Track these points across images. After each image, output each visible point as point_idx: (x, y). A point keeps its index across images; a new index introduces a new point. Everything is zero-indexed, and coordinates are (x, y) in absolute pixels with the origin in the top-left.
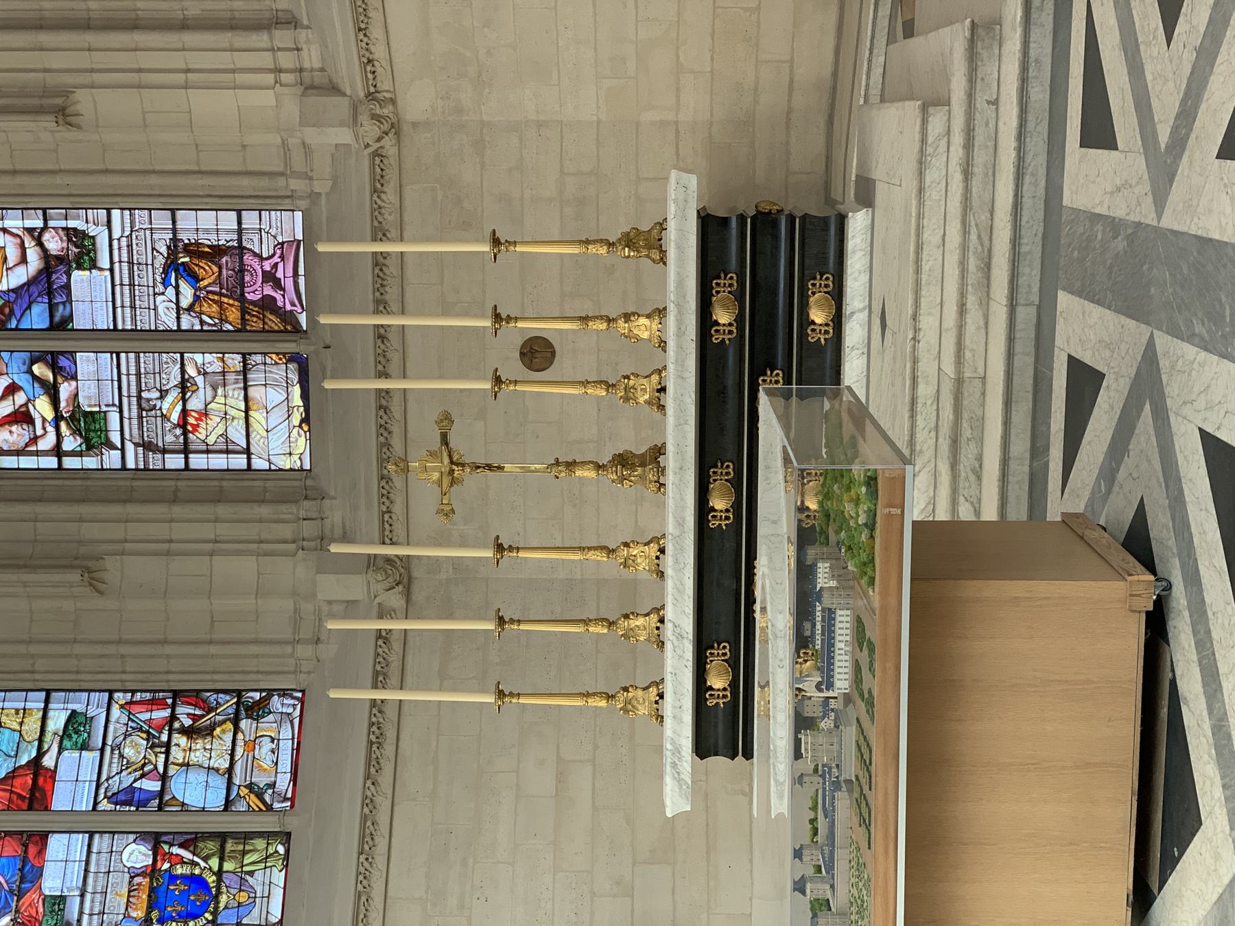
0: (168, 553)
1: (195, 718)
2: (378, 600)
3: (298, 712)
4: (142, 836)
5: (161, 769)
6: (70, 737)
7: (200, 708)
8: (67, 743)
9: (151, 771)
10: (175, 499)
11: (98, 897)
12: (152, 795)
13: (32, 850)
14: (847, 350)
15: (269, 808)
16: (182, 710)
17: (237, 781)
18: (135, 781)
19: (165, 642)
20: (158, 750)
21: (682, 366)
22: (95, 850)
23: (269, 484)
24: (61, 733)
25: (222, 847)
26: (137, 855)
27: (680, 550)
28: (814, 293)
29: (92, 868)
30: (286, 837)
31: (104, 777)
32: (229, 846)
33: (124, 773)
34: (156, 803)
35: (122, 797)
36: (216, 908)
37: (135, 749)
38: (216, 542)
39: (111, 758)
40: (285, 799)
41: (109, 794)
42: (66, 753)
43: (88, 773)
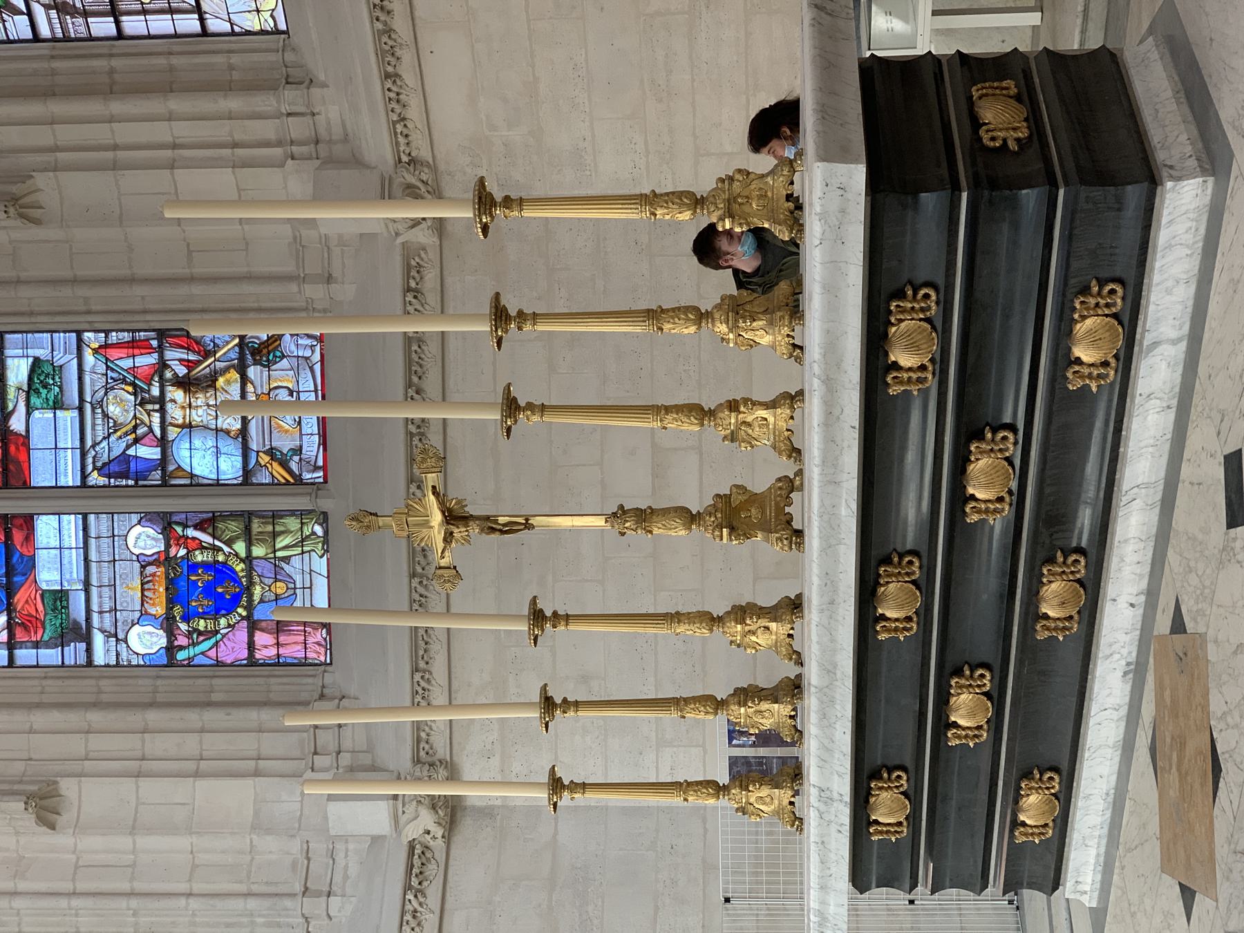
0: (115, 166)
1: (190, 365)
2: (400, 240)
3: (317, 357)
4: (147, 518)
5: (158, 432)
6: (38, 392)
7: (194, 351)
8: (35, 401)
9: (145, 435)
10: (112, 89)
11: (106, 592)
12: (151, 465)
13: (18, 536)
14: (1138, 400)
15: (299, 481)
16: (172, 355)
17: (254, 446)
18: (128, 447)
19: (132, 280)
20: (149, 407)
21: (835, 466)
22: (93, 533)
23: (235, 59)
24: (25, 388)
25: (248, 530)
26: (145, 540)
27: (828, 701)
28: (1084, 318)
29: (93, 556)
30: (324, 519)
31: (89, 443)
32: (256, 526)
33: (112, 438)
34: (157, 474)
35: (114, 468)
36: (250, 600)
37: (121, 406)
38: (175, 146)
39: (94, 418)
40: (316, 468)
41: (99, 464)
42: (37, 414)
43: (69, 439)
